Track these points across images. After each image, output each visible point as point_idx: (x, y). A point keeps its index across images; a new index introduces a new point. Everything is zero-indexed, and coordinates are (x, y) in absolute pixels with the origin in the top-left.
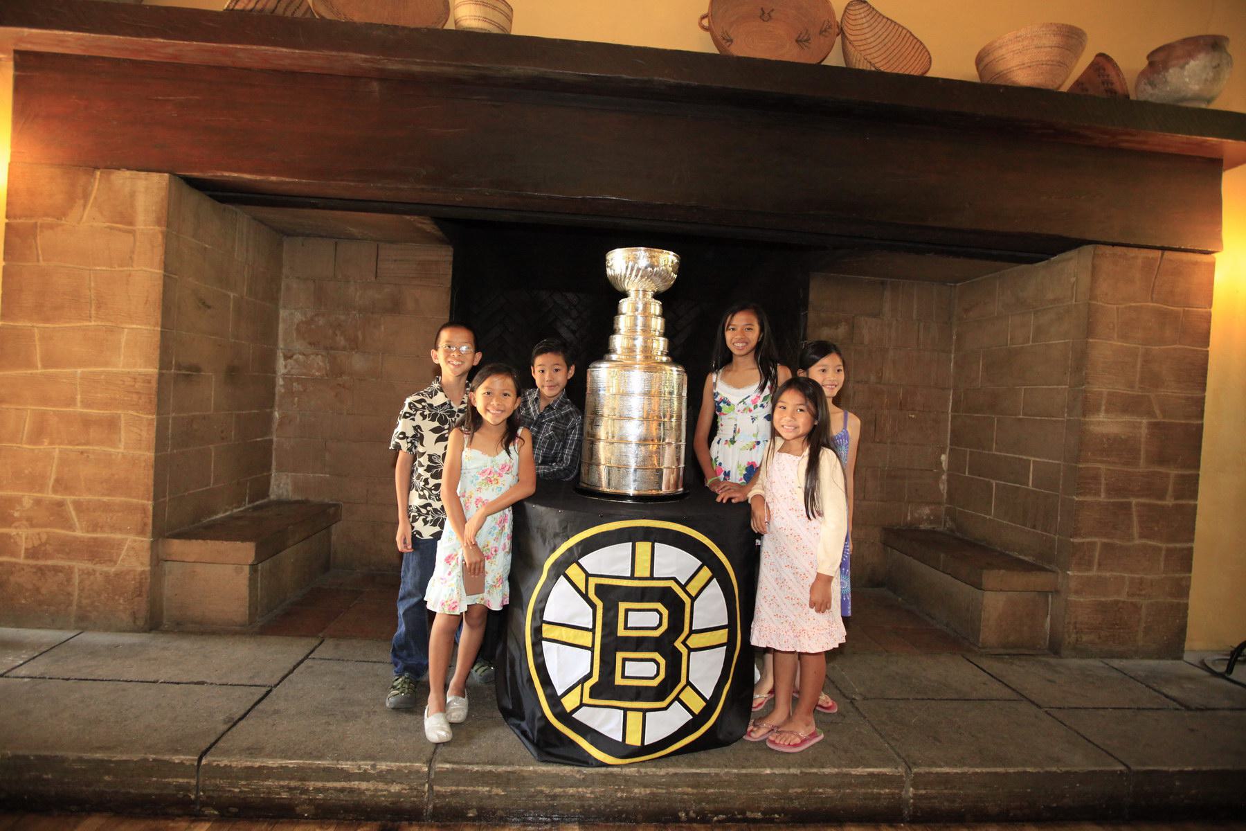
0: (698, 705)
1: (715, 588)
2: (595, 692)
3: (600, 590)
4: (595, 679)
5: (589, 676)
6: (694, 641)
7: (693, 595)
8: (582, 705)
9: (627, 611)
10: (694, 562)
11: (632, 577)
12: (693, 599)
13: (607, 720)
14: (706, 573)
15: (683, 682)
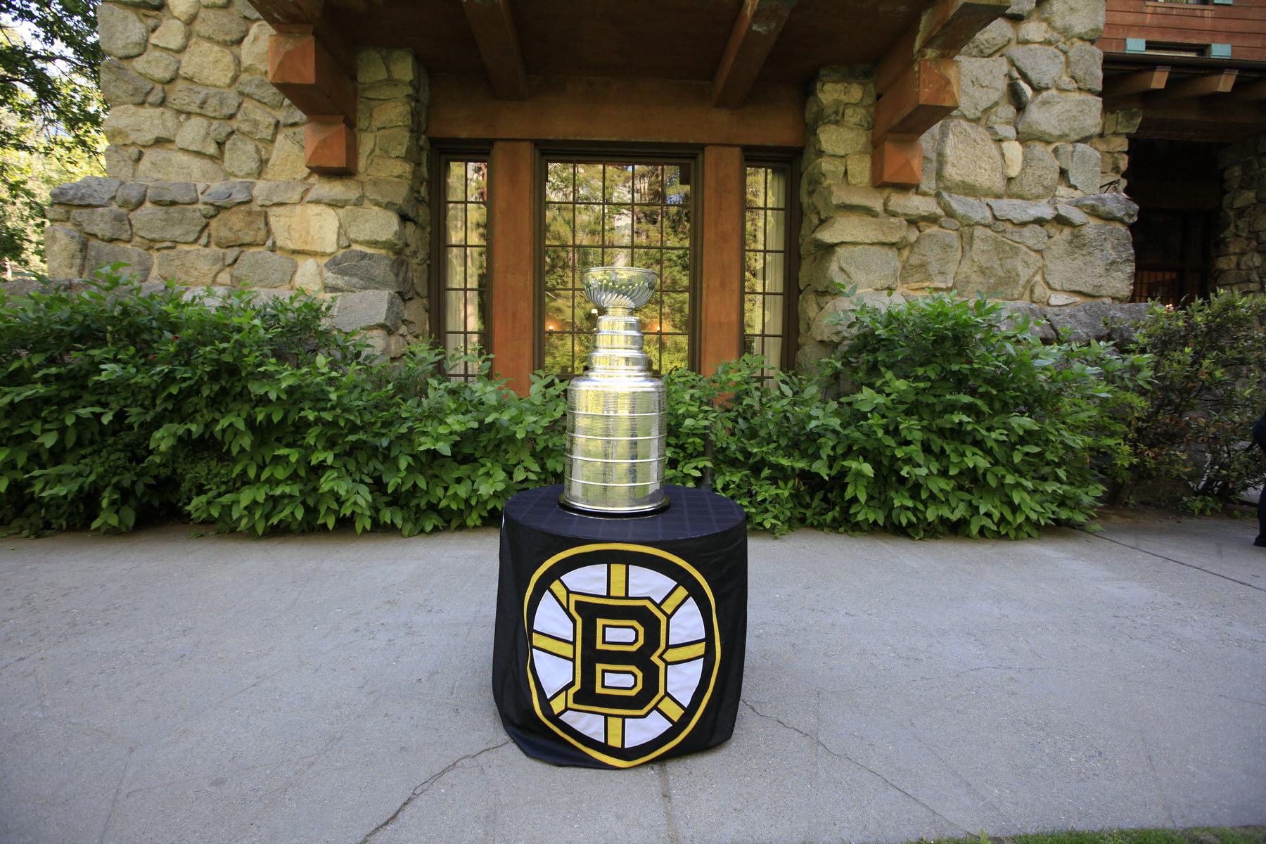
0: (676, 714)
1: (691, 606)
2: (578, 698)
3: (579, 605)
4: (578, 686)
5: (572, 684)
6: (671, 655)
7: (669, 612)
8: (567, 709)
9: (605, 627)
10: (668, 583)
11: (608, 596)
12: (669, 617)
13: (589, 723)
14: (682, 592)
15: (661, 692)
